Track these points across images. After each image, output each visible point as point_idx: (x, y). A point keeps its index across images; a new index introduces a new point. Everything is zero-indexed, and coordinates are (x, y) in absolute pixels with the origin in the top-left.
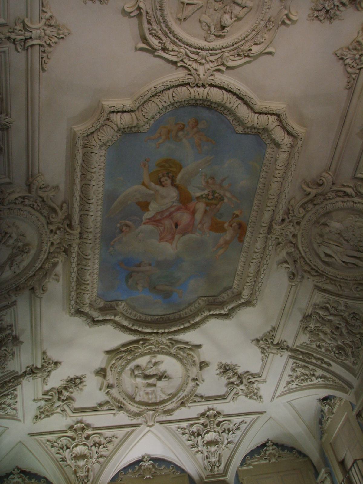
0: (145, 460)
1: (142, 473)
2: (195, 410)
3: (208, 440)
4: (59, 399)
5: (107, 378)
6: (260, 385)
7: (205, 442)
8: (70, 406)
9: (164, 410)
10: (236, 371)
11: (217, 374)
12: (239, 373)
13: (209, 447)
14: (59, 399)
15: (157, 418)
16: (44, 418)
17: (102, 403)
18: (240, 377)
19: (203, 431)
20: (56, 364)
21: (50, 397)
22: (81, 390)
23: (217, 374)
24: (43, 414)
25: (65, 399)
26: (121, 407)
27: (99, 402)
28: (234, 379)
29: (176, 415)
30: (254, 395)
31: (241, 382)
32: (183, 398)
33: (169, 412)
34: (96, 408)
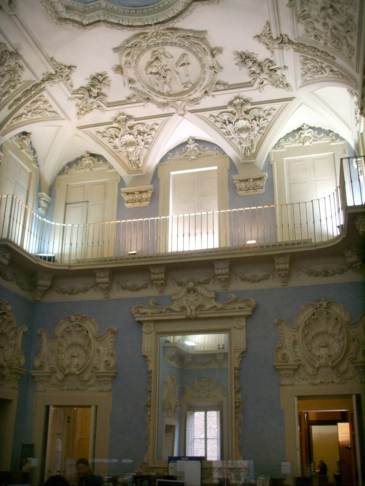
0: (190, 143)
1: (189, 155)
2: (223, 98)
3: (240, 127)
4: (90, 96)
5: (125, 73)
6: (284, 72)
7: (236, 129)
8: (103, 101)
9: (190, 99)
11: (236, 64)
12: (259, 62)
13: (240, 134)
14: (90, 96)
17: (130, 97)
20: (70, 67)
21: (82, 96)
22: (109, 85)
23: (236, 64)
24: (82, 111)
25: (96, 95)
27: (128, 96)
28: (253, 69)
29: (207, 102)
31: (262, 70)
32: (205, 87)
33: (195, 101)
34: (125, 101)
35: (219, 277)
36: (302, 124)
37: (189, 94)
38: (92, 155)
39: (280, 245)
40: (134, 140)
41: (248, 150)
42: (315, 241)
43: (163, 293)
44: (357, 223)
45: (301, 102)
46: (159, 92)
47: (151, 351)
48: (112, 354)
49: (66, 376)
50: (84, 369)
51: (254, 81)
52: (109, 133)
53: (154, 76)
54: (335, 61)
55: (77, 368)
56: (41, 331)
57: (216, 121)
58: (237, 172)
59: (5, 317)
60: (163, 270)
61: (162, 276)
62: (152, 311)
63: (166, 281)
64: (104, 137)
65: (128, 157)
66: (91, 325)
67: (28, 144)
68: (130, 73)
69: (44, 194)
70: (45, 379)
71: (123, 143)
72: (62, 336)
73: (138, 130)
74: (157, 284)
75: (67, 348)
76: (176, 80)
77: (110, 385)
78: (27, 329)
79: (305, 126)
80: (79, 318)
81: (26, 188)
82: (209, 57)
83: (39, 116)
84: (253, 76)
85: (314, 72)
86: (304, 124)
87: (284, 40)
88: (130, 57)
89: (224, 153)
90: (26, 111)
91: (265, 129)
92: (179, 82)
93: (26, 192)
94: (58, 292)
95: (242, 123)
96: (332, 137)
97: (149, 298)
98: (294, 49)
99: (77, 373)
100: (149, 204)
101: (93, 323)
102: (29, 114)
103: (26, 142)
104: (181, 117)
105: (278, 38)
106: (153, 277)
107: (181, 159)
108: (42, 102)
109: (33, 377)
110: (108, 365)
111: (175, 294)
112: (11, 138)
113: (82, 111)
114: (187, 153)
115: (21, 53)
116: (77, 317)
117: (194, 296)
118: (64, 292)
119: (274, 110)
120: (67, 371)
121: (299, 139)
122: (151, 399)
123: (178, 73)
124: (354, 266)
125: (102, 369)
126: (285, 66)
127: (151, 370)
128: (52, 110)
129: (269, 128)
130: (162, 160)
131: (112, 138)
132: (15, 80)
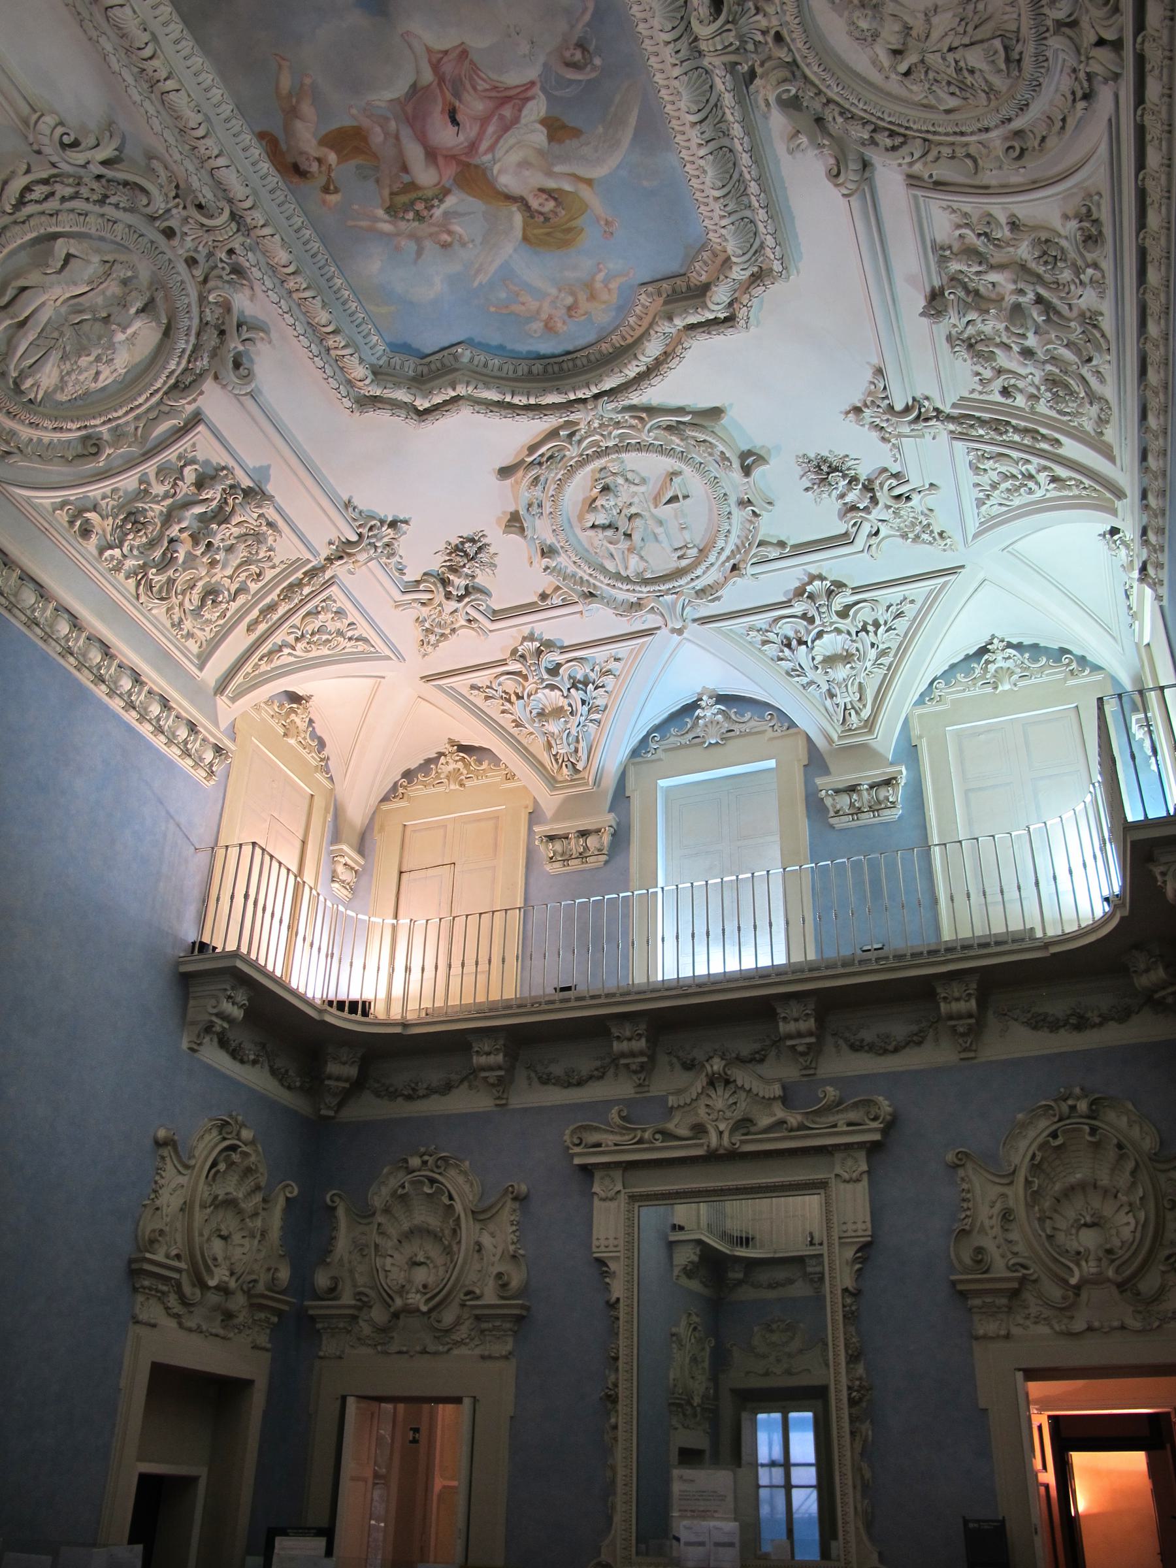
0: (703, 704)
3: (828, 654)
4: (448, 595)
5: (528, 533)
6: (931, 500)
7: (819, 658)
10: (852, 473)
11: (807, 489)
14: (448, 595)
15: (688, 609)
16: (438, 641)
18: (868, 488)
19: (808, 632)
20: (393, 524)
21: (429, 596)
23: (807, 489)
24: (434, 633)
26: (592, 595)
28: (851, 497)
30: (921, 531)
31: (874, 501)
35: (789, 1043)
36: (987, 638)
37: (693, 576)
38: (462, 748)
39: (949, 950)
40: (563, 702)
41: (853, 712)
42: (1045, 933)
43: (646, 1089)
44: (1157, 870)
45: (981, 576)
46: (618, 576)
47: (616, 1246)
48: (514, 1257)
49: (396, 1316)
50: (437, 1299)
51: (855, 529)
52: (500, 689)
53: (601, 534)
54: (1060, 451)
55: (425, 1294)
57: (765, 643)
58: (826, 771)
59: (235, 1157)
60: (642, 1028)
61: (642, 1044)
62: (618, 1138)
63: (652, 1058)
64: (487, 698)
65: (550, 746)
66: (461, 1180)
67: (302, 725)
68: (542, 528)
69: (345, 848)
70: (341, 1325)
71: (535, 712)
72: (387, 1211)
73: (570, 677)
74: (627, 1066)
75: (400, 1242)
76: (657, 540)
77: (510, 1340)
78: (296, 1192)
79: (995, 641)
80: (431, 1160)
81: (300, 835)
82: (737, 475)
83: (325, 651)
84: (852, 518)
85: (1008, 490)
86: (993, 637)
87: (923, 410)
88: (540, 487)
89: (792, 725)
90: (291, 639)
91: (891, 654)
92: (665, 544)
93: (298, 844)
94: (378, 1095)
95: (830, 644)
96: (1068, 665)
97: (609, 1104)
98: (952, 432)
99: (424, 1309)
100: (606, 862)
101: (465, 1173)
102: (299, 646)
103: (299, 721)
104: (676, 638)
105: (907, 410)
106: (617, 1047)
107: (683, 747)
108: (330, 616)
109: (313, 1319)
110: (504, 1286)
111: (679, 1092)
112: (257, 707)
113: (434, 633)
114: (698, 731)
115: (270, 489)
116: (426, 1158)
117: (727, 1096)
118: (393, 1095)
119: (912, 602)
120: (399, 1302)
121: (983, 676)
122: (617, 1379)
123: (660, 523)
124: (1157, 996)
125: (490, 1296)
126: (931, 485)
127: (618, 1300)
128: (356, 634)
129: (902, 650)
130: (635, 753)
131: (509, 701)
132: (259, 561)
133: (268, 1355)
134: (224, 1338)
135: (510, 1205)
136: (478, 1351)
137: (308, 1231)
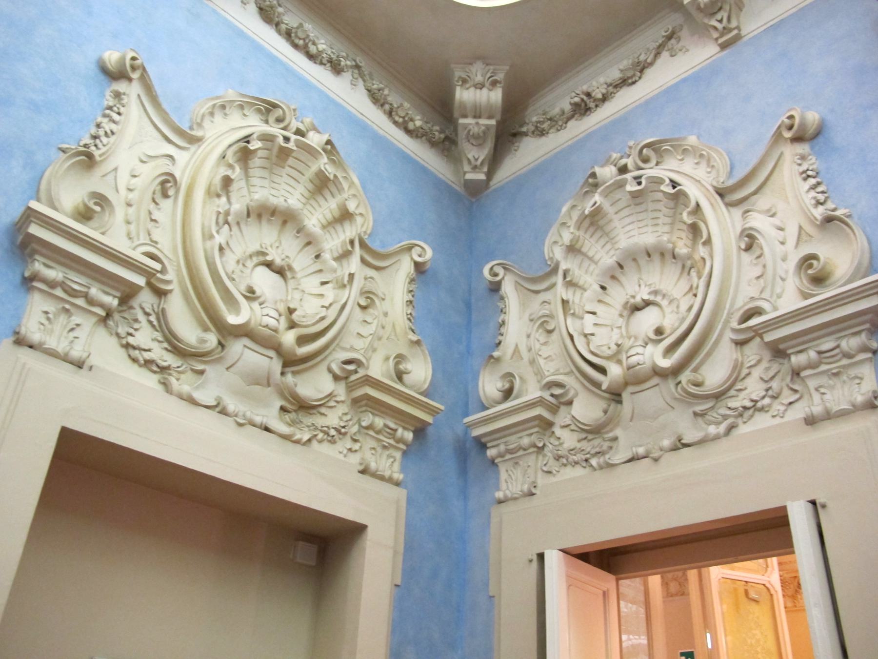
55: (660, 341)
56: (491, 269)
70: (526, 441)
75: (603, 288)
109: (481, 445)
118: (557, 122)
120: (615, 371)
133: (401, 494)
134: (286, 437)
135: (790, 152)
136: (798, 412)
137: (460, 313)
